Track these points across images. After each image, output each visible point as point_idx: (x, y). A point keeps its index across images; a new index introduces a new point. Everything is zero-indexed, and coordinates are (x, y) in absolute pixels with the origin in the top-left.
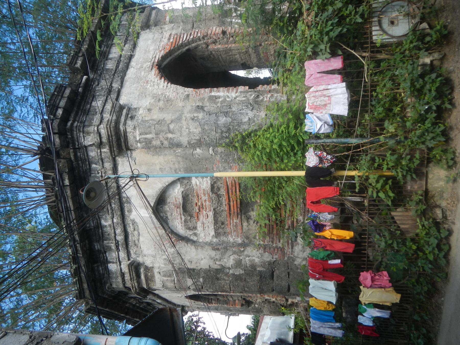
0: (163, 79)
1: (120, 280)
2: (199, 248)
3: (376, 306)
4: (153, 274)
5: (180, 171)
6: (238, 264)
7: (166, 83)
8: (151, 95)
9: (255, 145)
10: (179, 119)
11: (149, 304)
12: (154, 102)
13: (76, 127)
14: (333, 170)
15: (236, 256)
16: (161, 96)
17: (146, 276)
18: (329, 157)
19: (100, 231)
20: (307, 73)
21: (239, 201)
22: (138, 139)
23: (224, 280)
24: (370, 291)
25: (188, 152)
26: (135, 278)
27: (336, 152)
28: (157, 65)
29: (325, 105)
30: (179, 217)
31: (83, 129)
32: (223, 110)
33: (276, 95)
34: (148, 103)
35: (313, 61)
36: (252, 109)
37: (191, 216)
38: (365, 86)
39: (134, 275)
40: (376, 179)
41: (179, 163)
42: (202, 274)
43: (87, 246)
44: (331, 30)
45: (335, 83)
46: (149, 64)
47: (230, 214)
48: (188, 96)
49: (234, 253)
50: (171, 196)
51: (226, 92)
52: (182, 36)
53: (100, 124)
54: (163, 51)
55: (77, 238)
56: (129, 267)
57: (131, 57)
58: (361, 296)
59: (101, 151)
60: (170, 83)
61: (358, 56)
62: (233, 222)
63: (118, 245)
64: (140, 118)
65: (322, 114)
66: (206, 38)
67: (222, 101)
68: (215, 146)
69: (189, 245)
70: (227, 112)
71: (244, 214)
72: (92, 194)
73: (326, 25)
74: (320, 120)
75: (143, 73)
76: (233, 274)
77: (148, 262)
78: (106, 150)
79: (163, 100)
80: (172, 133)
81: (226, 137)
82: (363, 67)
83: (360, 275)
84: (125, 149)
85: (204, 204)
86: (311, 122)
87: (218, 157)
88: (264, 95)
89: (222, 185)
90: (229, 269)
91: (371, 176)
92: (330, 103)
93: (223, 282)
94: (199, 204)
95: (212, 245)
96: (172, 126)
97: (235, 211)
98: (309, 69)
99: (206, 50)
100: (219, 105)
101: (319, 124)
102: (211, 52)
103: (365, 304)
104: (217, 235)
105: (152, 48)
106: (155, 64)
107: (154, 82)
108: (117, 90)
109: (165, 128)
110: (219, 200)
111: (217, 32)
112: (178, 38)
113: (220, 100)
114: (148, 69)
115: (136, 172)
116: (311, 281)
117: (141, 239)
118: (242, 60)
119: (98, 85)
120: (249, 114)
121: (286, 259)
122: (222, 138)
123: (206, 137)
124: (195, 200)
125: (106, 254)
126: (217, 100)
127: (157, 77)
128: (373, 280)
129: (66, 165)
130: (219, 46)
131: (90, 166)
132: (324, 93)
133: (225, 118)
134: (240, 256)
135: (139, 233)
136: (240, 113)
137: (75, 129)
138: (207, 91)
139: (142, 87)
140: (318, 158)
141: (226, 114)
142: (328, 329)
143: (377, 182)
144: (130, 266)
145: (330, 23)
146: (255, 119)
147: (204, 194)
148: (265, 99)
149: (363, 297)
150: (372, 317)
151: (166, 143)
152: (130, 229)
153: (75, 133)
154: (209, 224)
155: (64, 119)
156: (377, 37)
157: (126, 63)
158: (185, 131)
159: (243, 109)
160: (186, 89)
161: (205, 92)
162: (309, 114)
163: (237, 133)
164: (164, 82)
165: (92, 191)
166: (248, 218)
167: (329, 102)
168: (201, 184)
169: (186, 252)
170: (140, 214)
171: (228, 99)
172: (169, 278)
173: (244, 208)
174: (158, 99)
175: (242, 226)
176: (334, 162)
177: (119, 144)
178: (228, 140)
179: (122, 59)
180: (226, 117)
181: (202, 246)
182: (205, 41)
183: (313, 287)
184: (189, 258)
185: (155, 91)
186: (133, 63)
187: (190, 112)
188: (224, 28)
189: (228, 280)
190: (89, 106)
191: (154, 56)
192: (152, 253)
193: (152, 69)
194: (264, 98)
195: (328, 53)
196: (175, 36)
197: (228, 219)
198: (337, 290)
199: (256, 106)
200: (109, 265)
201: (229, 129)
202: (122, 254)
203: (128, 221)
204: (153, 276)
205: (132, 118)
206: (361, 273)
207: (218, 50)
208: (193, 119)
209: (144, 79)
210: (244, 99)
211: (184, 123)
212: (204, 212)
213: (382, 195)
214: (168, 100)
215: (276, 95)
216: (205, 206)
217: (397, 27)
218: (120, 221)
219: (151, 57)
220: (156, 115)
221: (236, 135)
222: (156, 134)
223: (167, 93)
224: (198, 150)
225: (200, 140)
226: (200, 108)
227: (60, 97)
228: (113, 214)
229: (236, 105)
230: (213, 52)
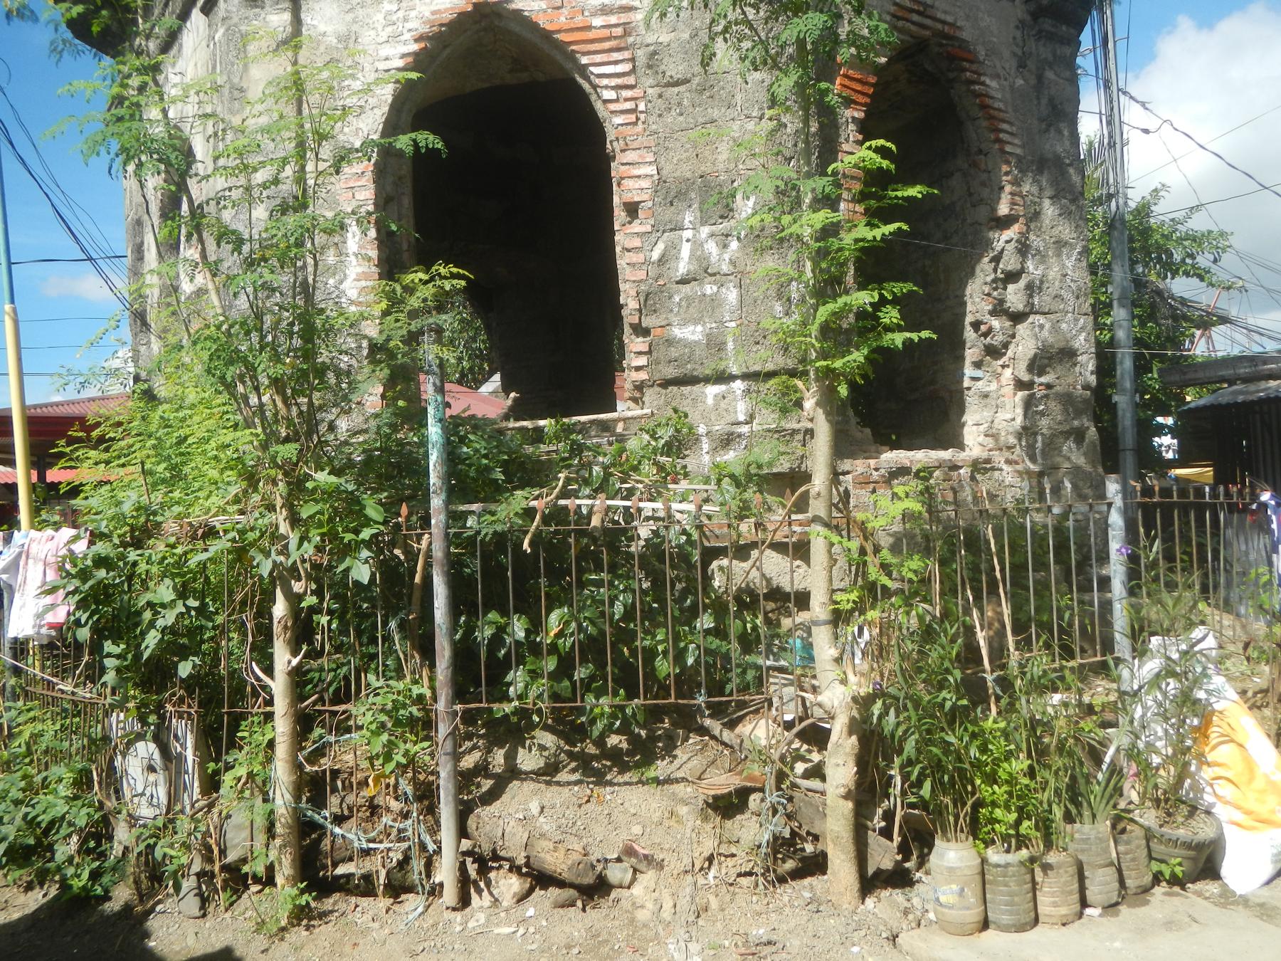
0: (415, 47)
8: (355, 28)
16: (349, 63)
34: (322, 28)
52: (616, 56)
112: (607, 45)
127: (429, 21)
164: (403, 56)
188: (650, 204)
196: (619, 31)
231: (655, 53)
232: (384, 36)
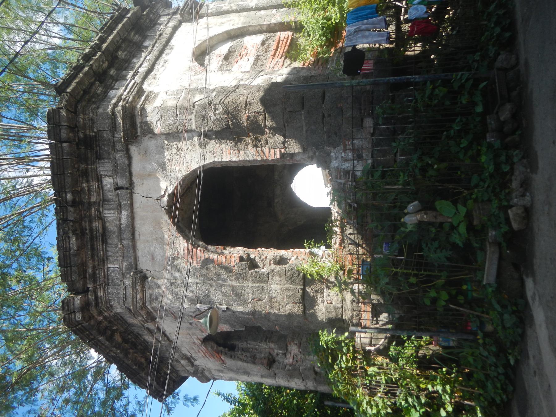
19: (127, 64)
21: (287, 47)
26: (134, 93)
55: (104, 47)
63: (137, 74)
85: (249, 52)
89: (274, 43)
97: (281, 53)
125: (116, 82)
147: (253, 46)
153: (159, 5)
228: (150, 53)
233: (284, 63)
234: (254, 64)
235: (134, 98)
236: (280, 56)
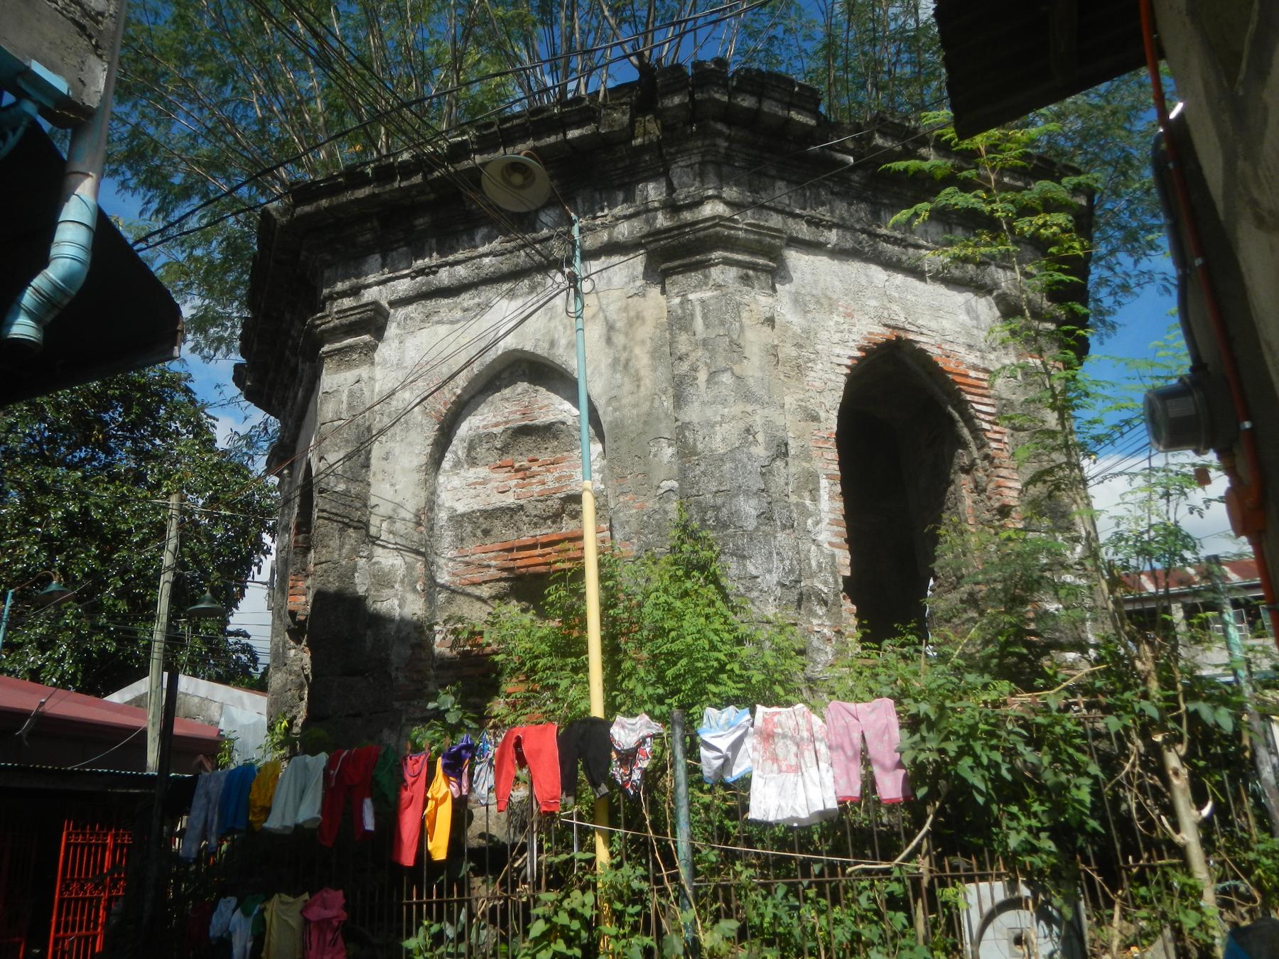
0: (858, 354)
1: (340, 286)
2: (422, 476)
3: (259, 938)
4: (357, 366)
5: (615, 410)
6: (383, 580)
7: (849, 362)
8: (813, 325)
9: (686, 594)
10: (748, 397)
11: (294, 372)
12: (794, 334)
13: (715, 145)
14: (604, 789)
15: (401, 572)
17: (351, 348)
18: (636, 776)
20: (860, 706)
21: (543, 569)
22: (691, 297)
23: (342, 546)
24: (295, 922)
25: (662, 426)
26: (344, 321)
27: (648, 790)
28: (899, 338)
29: (775, 759)
30: (500, 419)
31: (712, 162)
32: (776, 509)
33: (829, 649)
34: (789, 317)
35: (894, 721)
36: (784, 585)
37: (504, 450)
38: (832, 866)
39: (353, 318)
40: (580, 910)
41: (636, 405)
42: (355, 489)
43: (423, 198)
44: (978, 763)
45: (835, 782)
46: (900, 319)
47: (510, 550)
48: (815, 418)
49: (410, 568)
50: (552, 395)
51: (832, 516)
52: (986, 400)
53: (727, 203)
54: (939, 352)
56: (372, 303)
57: (917, 272)
58: (285, 898)
59: (656, 209)
60: (848, 371)
61: (914, 843)
62: (490, 559)
63: (427, 275)
64: (747, 299)
65: (750, 751)
66: (986, 463)
67: (804, 506)
68: (684, 496)
69: (429, 449)
70: (770, 519)
71: (511, 587)
72: (517, 179)
73: (995, 748)
74: (736, 746)
75: (873, 303)
76: (354, 569)
77: (386, 351)
78: (662, 221)
79: (799, 357)
80: (708, 381)
81: (703, 521)
82: (887, 857)
83: (337, 890)
84: (663, 266)
85: (534, 480)
86: (729, 724)
87: (651, 504)
88: (830, 619)
90: (370, 557)
91: (589, 898)
92: (780, 771)
93: (335, 543)
94: (535, 468)
95: (431, 509)
96: (726, 378)
97: (519, 563)
98: (873, 710)
99: (957, 467)
100: (793, 499)
101: (723, 744)
102: (953, 481)
103: (262, 911)
104: (458, 520)
105: (947, 324)
106: (902, 334)
107: (850, 332)
108: (822, 239)
109: (721, 362)
110: (545, 519)
111: (1006, 491)
112: (980, 391)
113: (808, 502)
114: (886, 315)
115: (586, 286)
116: (323, 757)
117: (443, 330)
118: (942, 568)
119: (832, 193)
120: (768, 576)
121: (397, 705)
122: (703, 510)
123: (702, 469)
124: (545, 457)
126: (806, 494)
127: (865, 338)
128: (323, 924)
129: (616, 128)
130: (968, 502)
131: (620, 187)
132: (806, 754)
133: (754, 513)
134: (402, 582)
135: (458, 321)
136: (771, 553)
137: (707, 142)
138: (831, 467)
139: (837, 304)
140: (633, 745)
141: (766, 517)
142: (203, 816)
143: (573, 914)
144: (375, 305)
145: (997, 756)
146: (755, 594)
147: (559, 479)
148: (815, 622)
149: (282, 903)
150: (230, 935)
151: (684, 367)
152: (467, 299)
153: (699, 143)
154: (483, 496)
155: (729, 114)
156: (976, 898)
157: (899, 260)
158: (716, 413)
159: (782, 561)
160: (836, 413)
161: (827, 463)
162: (748, 717)
163: (717, 548)
164: (850, 358)
165: (525, 179)
166: (501, 597)
167: (784, 768)
168: (585, 470)
169: (410, 444)
170: (507, 319)
171: (810, 522)
172: (344, 406)
173: (527, 587)
174: (801, 342)
175: (480, 584)
176: (626, 793)
177: (672, 255)
178: (696, 524)
179: (911, 250)
180: (758, 516)
181: (426, 481)
182: (978, 461)
183: (306, 766)
184: (397, 451)
185: (823, 335)
186: (899, 278)
187: (768, 423)
189: (340, 555)
190: (773, 172)
191: (925, 331)
192: (407, 358)
193: (885, 325)
194: (820, 617)
195: (916, 758)
196: (985, 384)
197: (498, 546)
198: (298, 827)
199: (794, 596)
200: (377, 256)
201: (725, 526)
202: (403, 286)
203: (487, 293)
204: (350, 365)
205: (745, 279)
206: (341, 893)
207: (959, 500)
208: (748, 431)
209: (856, 307)
210: (814, 564)
211: (737, 409)
212: (513, 482)
213: (538, 928)
214: (800, 369)
215: (829, 649)
216: (531, 484)
217: (1007, 953)
218: (483, 273)
219: (920, 322)
220: (755, 339)
221: (711, 547)
222: (704, 340)
223: (820, 366)
224: (670, 451)
225: (694, 452)
226: (781, 451)
227: (787, 99)
228: (502, 254)
229: (792, 542)
230: (952, 488)
231: (1005, 405)
232: (836, 337)
233: (486, 582)
234: (490, 514)
235: (335, 328)
236: (511, 564)
